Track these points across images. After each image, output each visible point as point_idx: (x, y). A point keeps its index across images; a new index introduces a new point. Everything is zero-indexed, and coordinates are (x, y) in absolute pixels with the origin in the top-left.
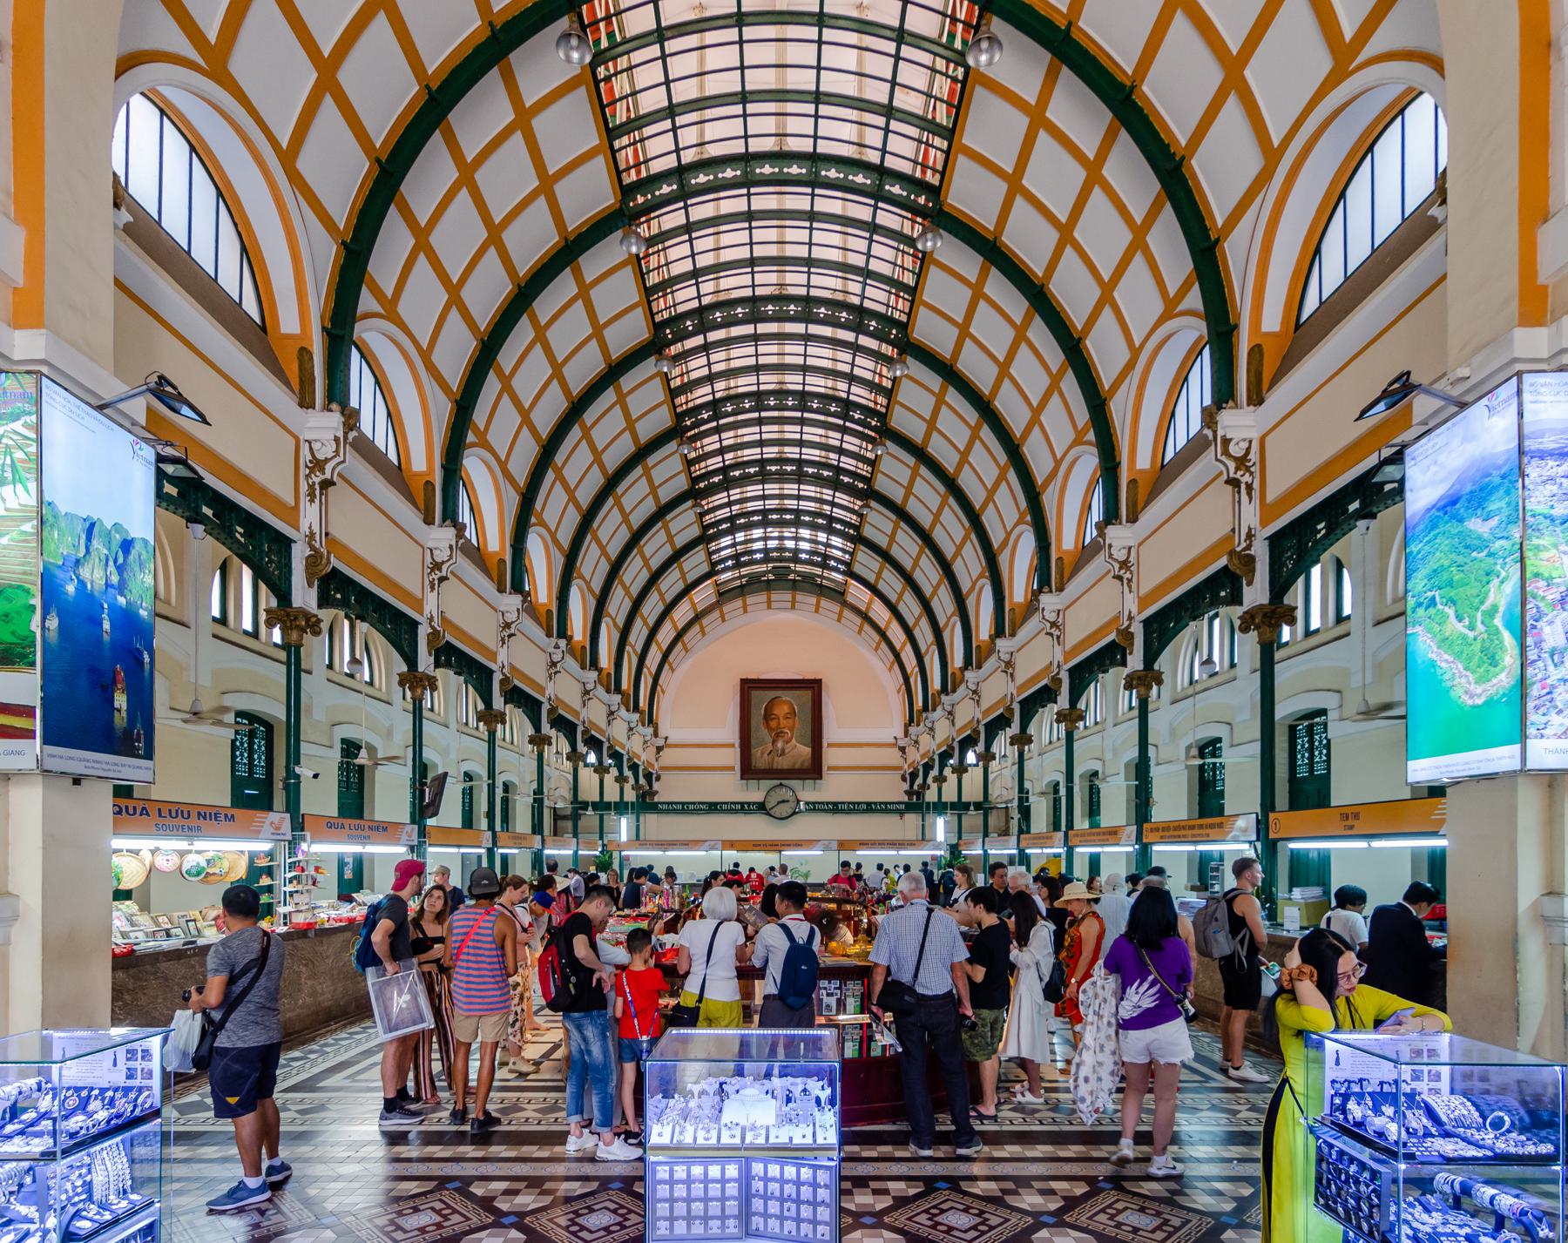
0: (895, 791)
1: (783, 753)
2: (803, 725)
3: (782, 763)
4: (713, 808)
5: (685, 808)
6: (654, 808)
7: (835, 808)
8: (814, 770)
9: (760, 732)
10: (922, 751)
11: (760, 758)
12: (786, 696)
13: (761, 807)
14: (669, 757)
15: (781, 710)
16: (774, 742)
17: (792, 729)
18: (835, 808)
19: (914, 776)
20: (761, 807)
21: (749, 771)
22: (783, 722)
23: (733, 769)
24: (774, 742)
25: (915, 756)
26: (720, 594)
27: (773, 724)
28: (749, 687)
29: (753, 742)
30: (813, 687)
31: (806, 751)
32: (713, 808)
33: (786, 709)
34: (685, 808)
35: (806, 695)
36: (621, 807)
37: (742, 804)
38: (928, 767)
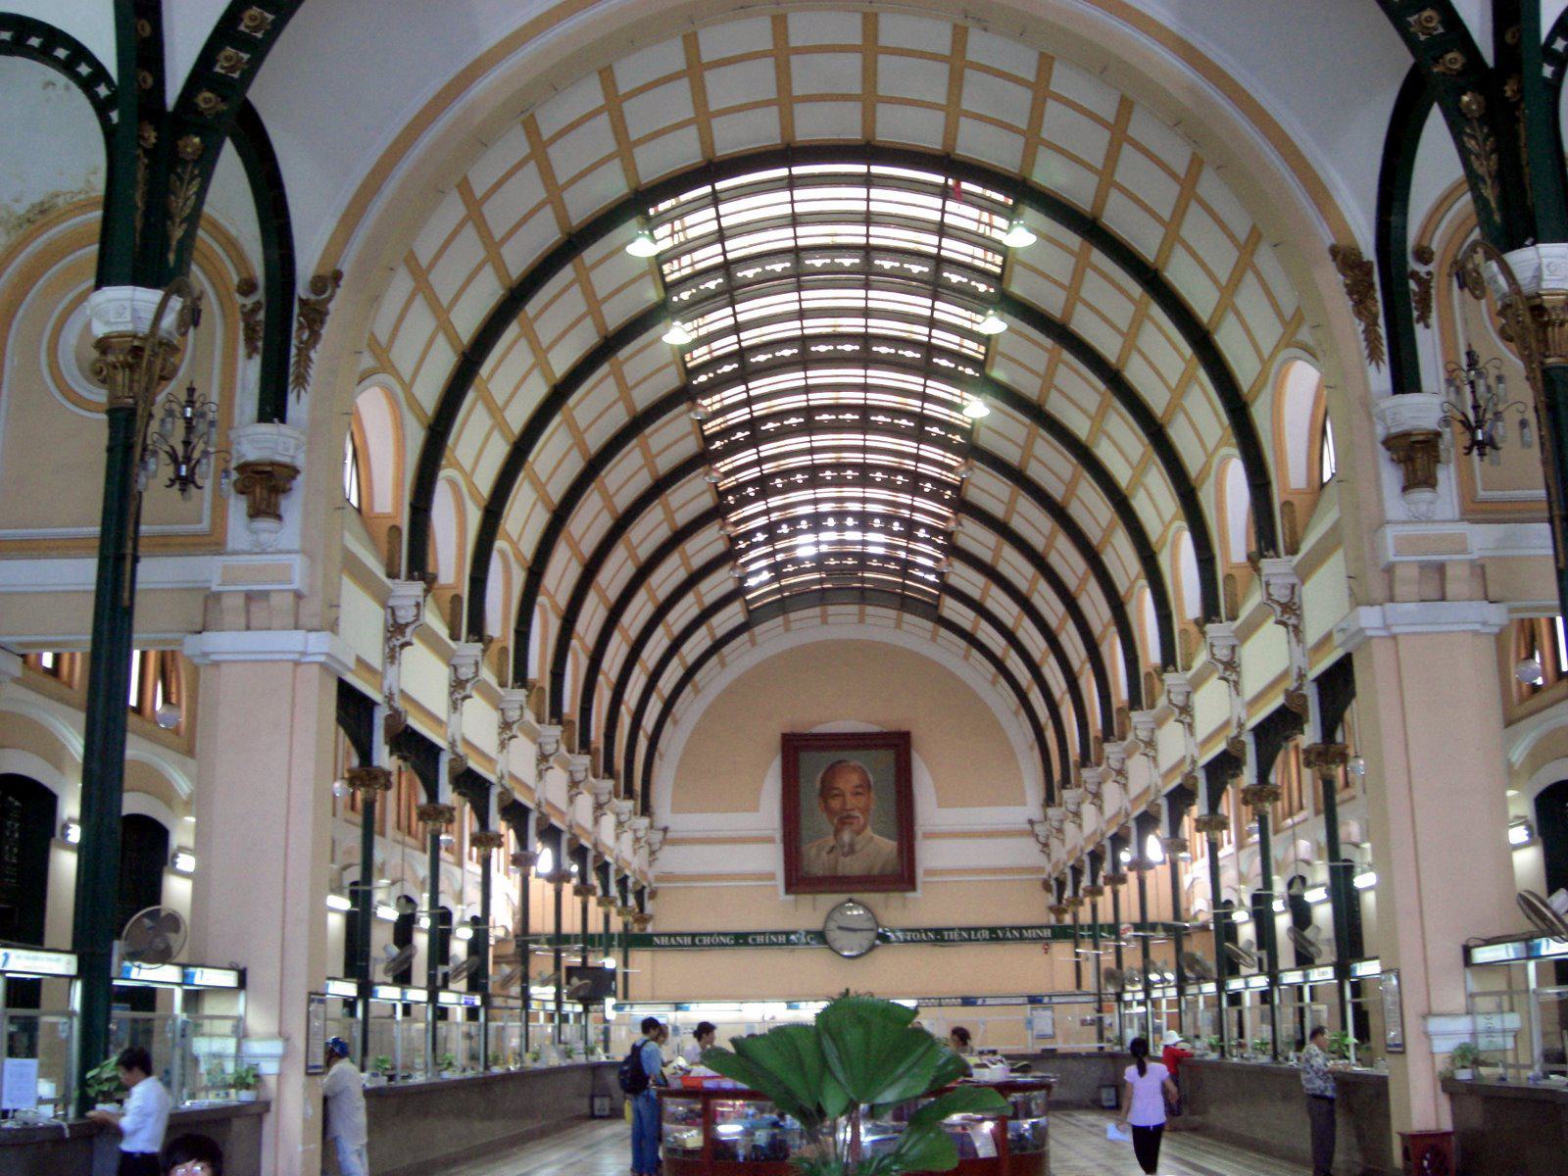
0: (1034, 909)
1: (852, 850)
2: (881, 802)
3: (852, 866)
4: (741, 939)
5: (695, 941)
6: (645, 941)
7: (938, 936)
8: (902, 876)
9: (815, 820)
10: (1069, 845)
11: (817, 859)
12: (856, 758)
13: (820, 937)
14: (673, 860)
15: (848, 782)
16: (837, 832)
17: (865, 811)
18: (938, 936)
19: (1061, 885)
20: (820, 937)
21: (798, 879)
22: (852, 802)
23: (771, 876)
24: (837, 832)
25: (1063, 854)
26: (750, 612)
27: (835, 804)
28: (795, 747)
29: (804, 834)
30: (898, 745)
31: (888, 846)
32: (741, 939)
33: (854, 779)
34: (695, 941)
35: (887, 757)
36: (604, 941)
37: (787, 934)
38: (1077, 872)
